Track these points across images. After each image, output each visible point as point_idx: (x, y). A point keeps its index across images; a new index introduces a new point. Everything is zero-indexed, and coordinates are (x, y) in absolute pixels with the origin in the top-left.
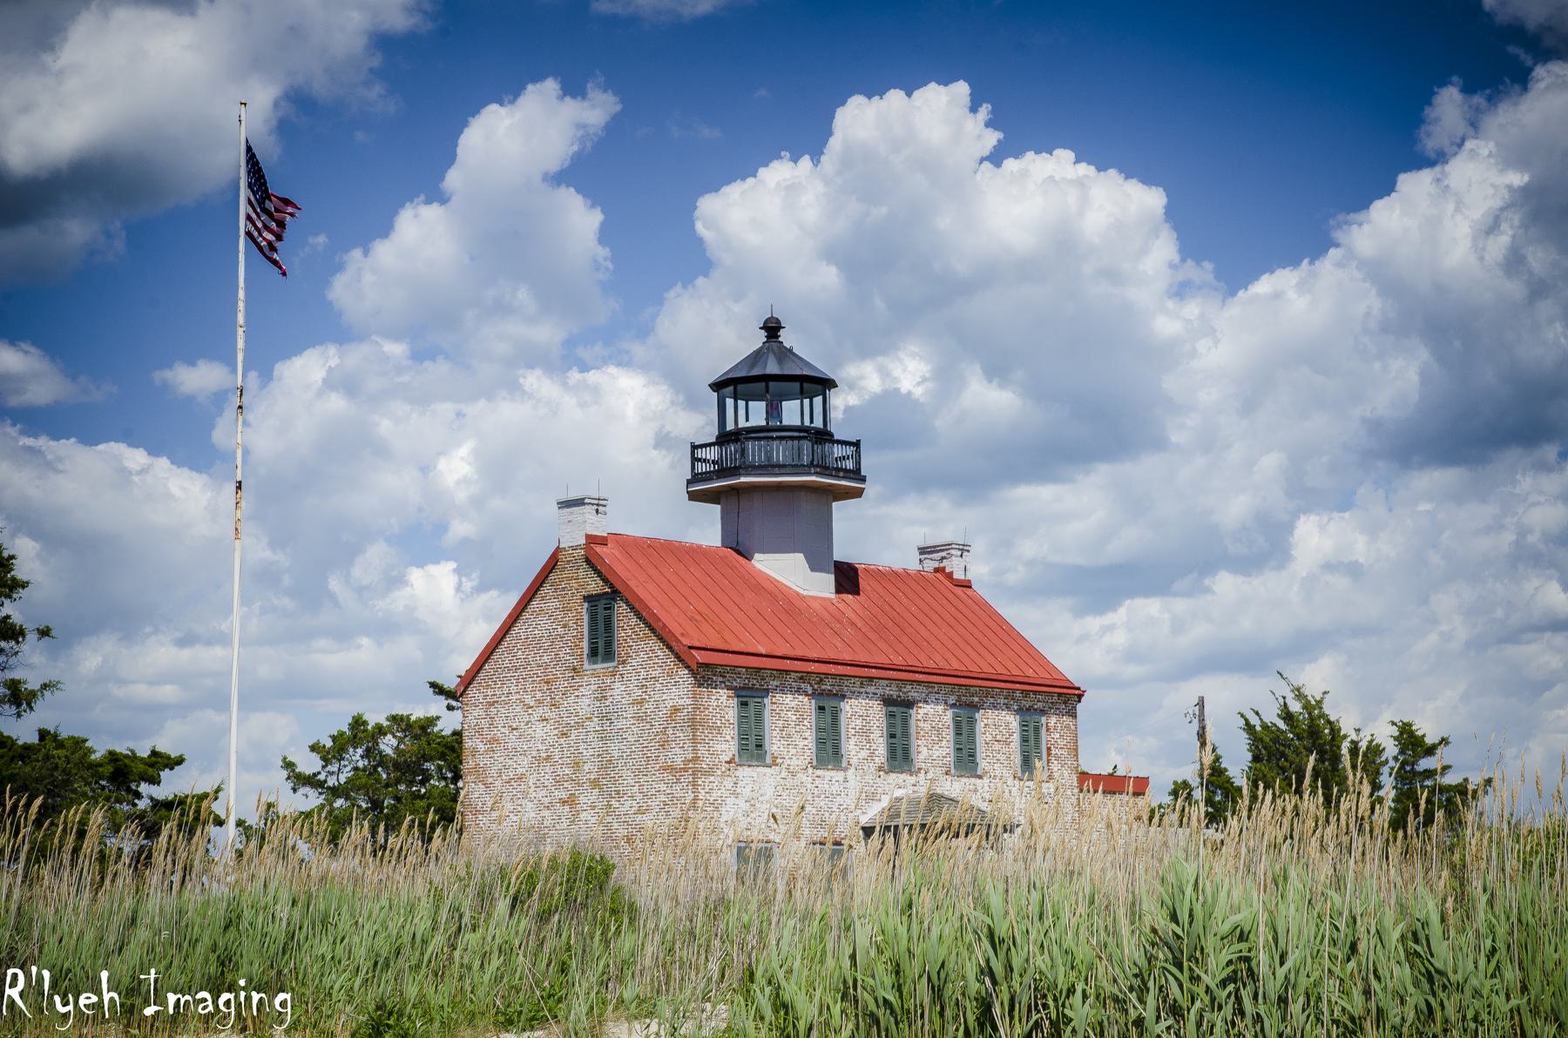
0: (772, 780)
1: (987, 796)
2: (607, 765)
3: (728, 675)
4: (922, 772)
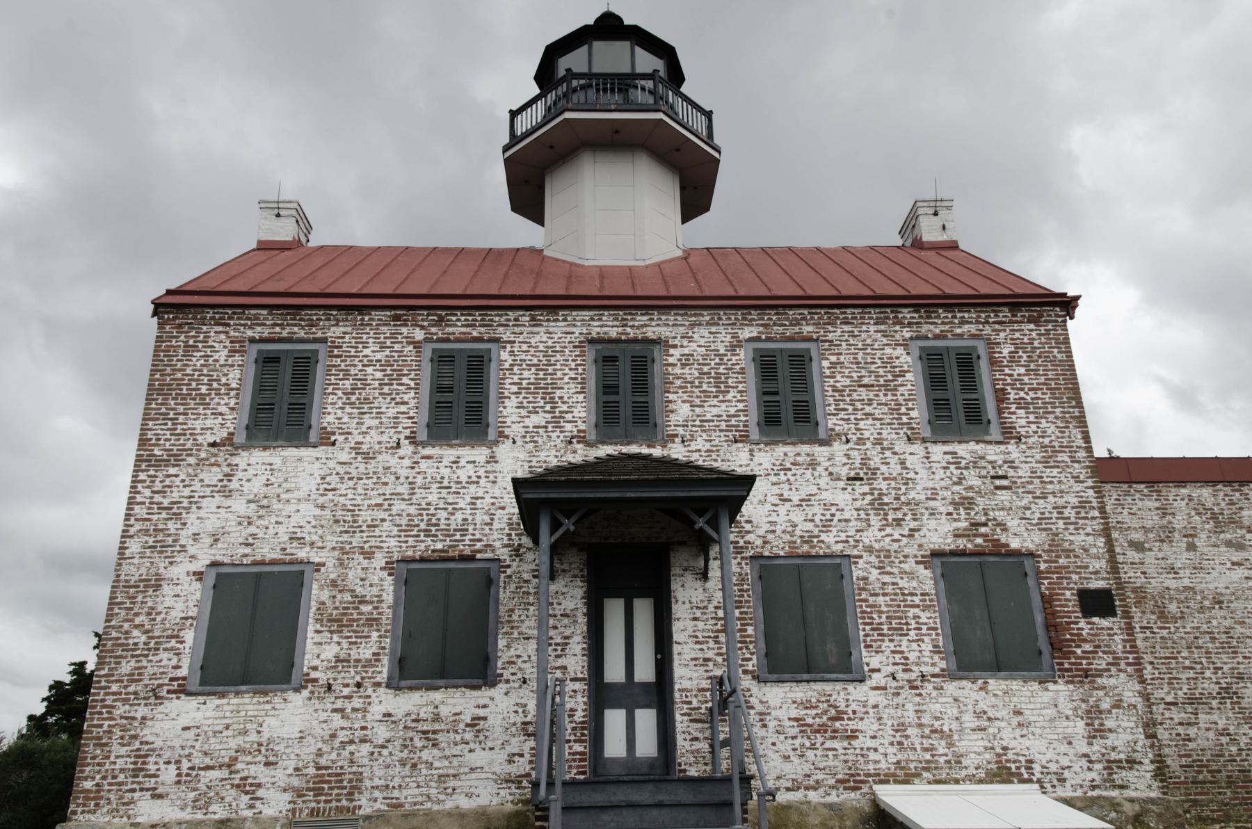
0: (318, 465)
1: (844, 472)
3: (232, 323)
4: (678, 440)
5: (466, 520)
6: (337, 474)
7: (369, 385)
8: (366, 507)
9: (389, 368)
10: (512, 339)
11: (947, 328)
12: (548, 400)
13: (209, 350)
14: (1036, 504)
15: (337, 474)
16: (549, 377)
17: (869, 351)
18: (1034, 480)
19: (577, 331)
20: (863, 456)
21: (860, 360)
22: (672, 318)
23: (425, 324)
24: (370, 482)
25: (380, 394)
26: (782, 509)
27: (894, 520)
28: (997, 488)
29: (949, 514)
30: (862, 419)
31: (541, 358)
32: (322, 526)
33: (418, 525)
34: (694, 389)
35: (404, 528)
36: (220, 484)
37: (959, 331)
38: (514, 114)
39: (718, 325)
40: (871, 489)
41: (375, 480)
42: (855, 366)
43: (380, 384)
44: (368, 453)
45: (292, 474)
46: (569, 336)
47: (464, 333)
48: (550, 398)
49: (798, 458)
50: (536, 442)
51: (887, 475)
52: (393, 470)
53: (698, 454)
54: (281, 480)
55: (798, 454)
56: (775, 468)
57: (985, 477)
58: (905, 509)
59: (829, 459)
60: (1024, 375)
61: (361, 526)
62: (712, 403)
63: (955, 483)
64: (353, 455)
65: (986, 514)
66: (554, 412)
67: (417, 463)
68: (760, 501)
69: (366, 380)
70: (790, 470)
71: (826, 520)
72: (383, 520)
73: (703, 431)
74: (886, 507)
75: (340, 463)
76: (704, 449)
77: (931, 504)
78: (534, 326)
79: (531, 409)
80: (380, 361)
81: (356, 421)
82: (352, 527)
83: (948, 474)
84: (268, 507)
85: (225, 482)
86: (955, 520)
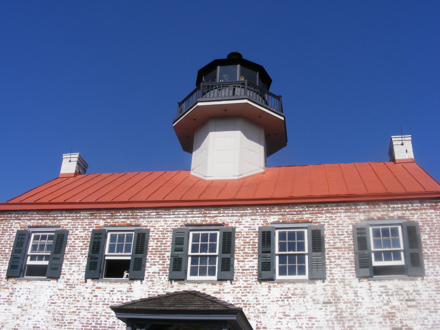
0: (49, 290)
1: (322, 299)
3: (22, 218)
5: (114, 322)
6: (57, 295)
7: (76, 249)
8: (68, 313)
9: (86, 241)
10: (146, 225)
11: (385, 213)
12: (161, 258)
13: (11, 231)
14: (431, 316)
15: (57, 295)
16: (163, 245)
17: (340, 228)
18: (430, 302)
19: (180, 220)
20: (333, 289)
21: (335, 233)
22: (231, 212)
23: (105, 217)
24: (71, 300)
25: (81, 254)
26: (284, 321)
27: (348, 327)
28: (409, 306)
29: (381, 323)
30: (334, 268)
31: (160, 235)
32: (48, 322)
33: (91, 324)
34: (240, 252)
35: (85, 325)
36: (8, 298)
37: (391, 215)
38: (180, 104)
39: (256, 215)
40: (336, 309)
41: (73, 299)
42: (332, 237)
43: (81, 249)
44: (72, 285)
45: (37, 294)
46: (175, 223)
47: (123, 222)
48: (163, 257)
49: (296, 291)
50: (153, 281)
51: (346, 300)
52: (82, 294)
53: (239, 288)
54: (33, 297)
55: (296, 289)
56: (282, 297)
57: (402, 300)
58: (355, 320)
59: (314, 292)
60: (428, 239)
61: (65, 323)
62: (250, 260)
63: (385, 304)
64: (65, 286)
65: (401, 323)
66: (164, 265)
67: (94, 291)
68: (272, 316)
69: (75, 246)
70: (291, 298)
71: (309, 327)
72: (75, 320)
73: (243, 276)
74: (344, 319)
75: (59, 289)
76: (243, 286)
77: (370, 317)
78: (158, 218)
79: (152, 263)
80: (82, 237)
81: (68, 267)
82: (61, 323)
83: (381, 299)
84: (26, 310)
85: (10, 297)
86: (384, 326)
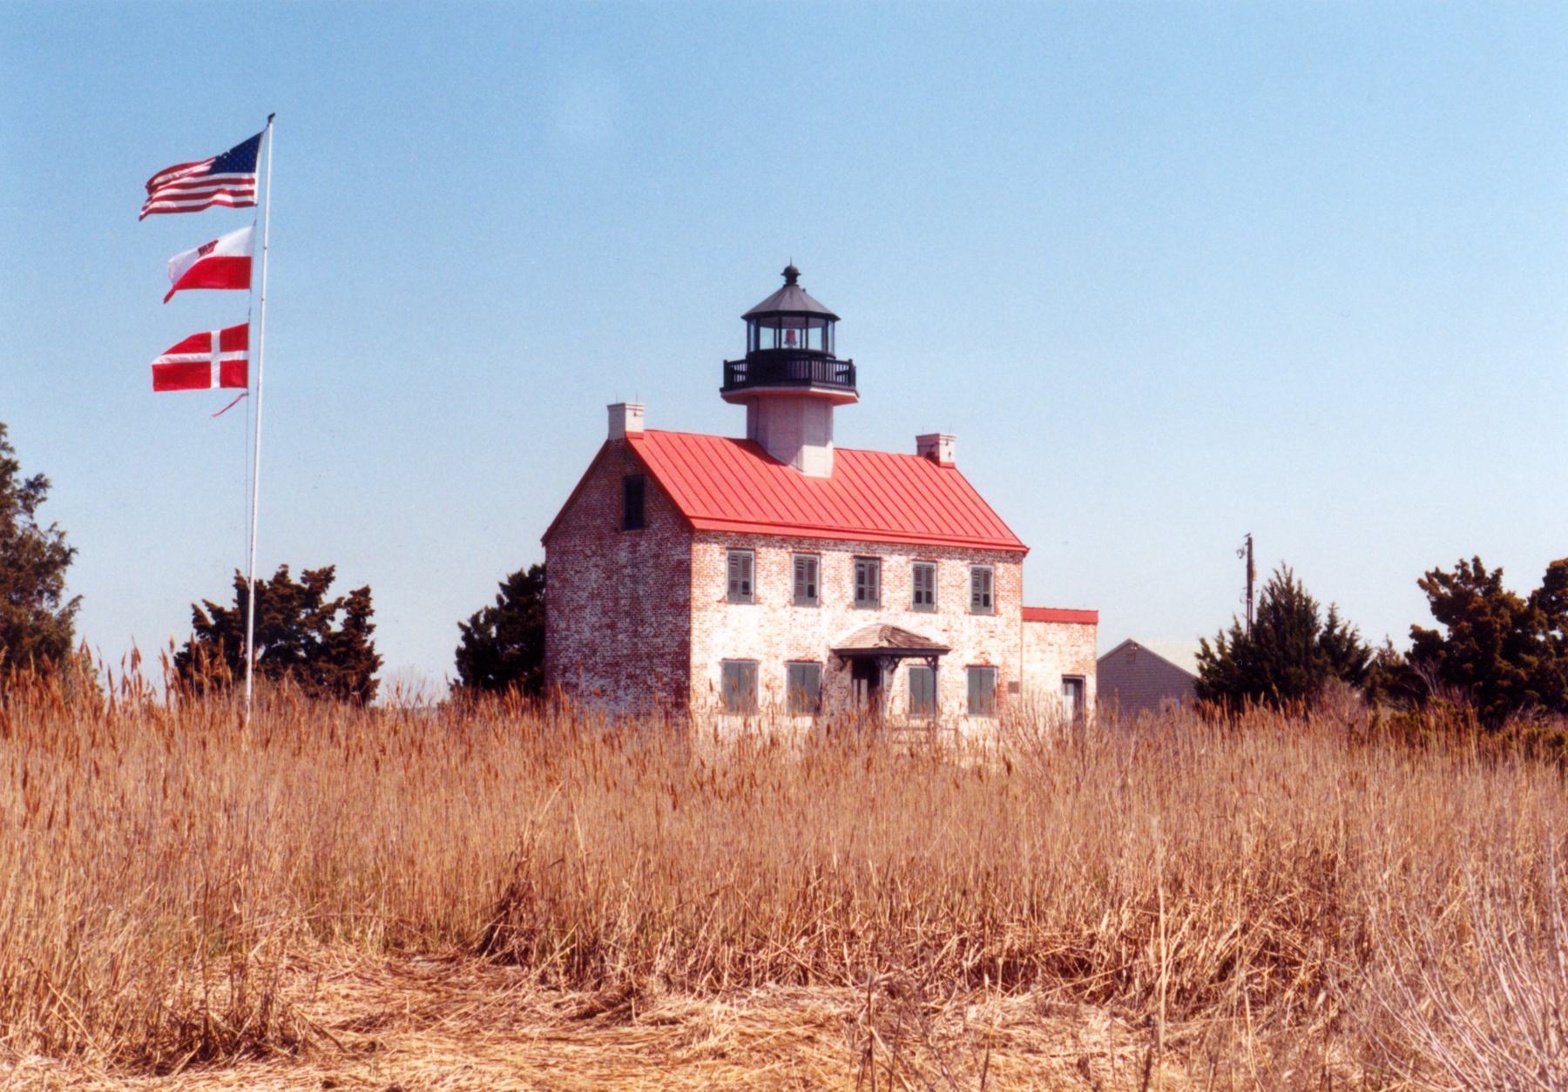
2: (635, 600)
